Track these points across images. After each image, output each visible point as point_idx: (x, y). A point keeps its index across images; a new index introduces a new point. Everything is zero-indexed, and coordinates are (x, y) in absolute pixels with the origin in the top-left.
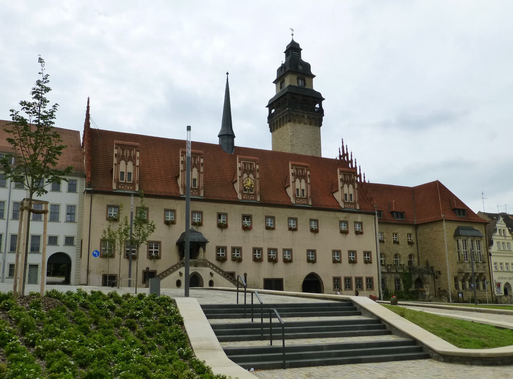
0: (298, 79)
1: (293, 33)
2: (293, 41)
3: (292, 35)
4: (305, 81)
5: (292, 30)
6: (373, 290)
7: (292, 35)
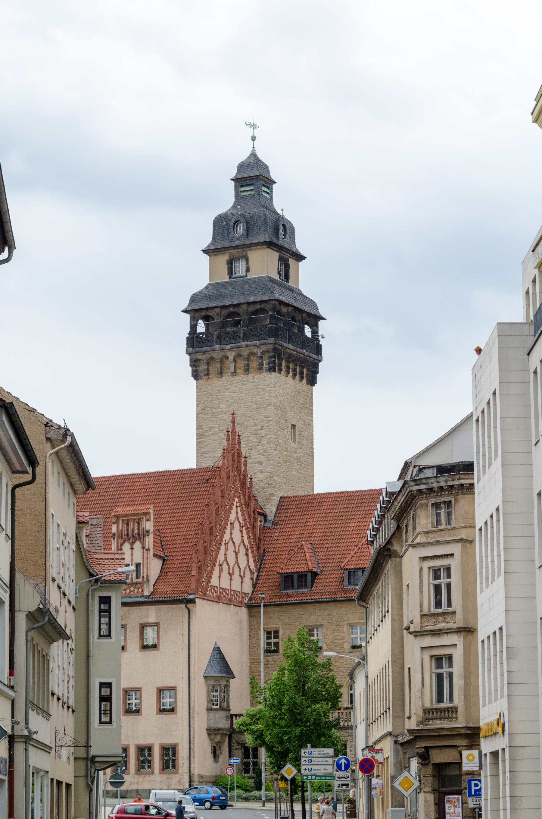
0: (230, 263)
1: (257, 132)
2: (253, 155)
3: (253, 139)
4: (247, 263)
5: (253, 126)
6: (177, 773)
7: (253, 139)
